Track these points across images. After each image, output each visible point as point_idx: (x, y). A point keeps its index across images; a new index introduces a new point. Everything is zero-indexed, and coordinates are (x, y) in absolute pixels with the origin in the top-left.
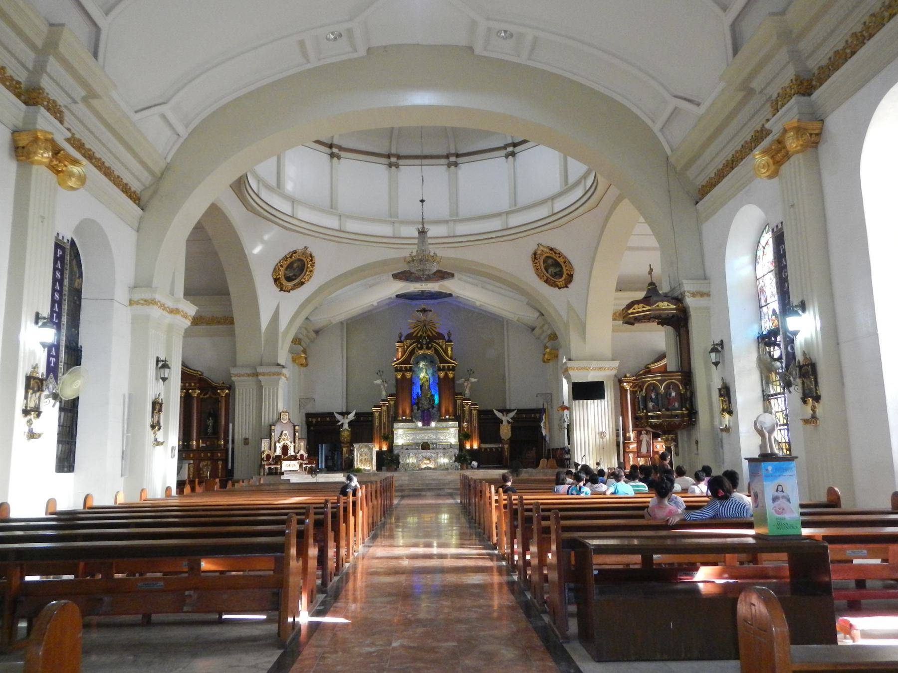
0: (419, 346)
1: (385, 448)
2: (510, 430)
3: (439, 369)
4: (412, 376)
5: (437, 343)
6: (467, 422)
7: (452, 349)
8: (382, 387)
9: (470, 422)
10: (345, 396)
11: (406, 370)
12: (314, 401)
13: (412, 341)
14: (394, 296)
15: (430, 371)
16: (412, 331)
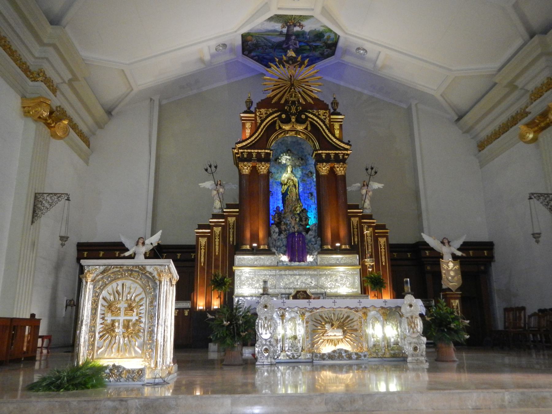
0: (284, 116)
1: (216, 304)
2: (459, 272)
3: (319, 159)
4: (269, 172)
5: (312, 114)
6: (371, 257)
7: (341, 126)
8: (215, 192)
9: (376, 257)
10: (150, 215)
11: (260, 159)
12: (68, 199)
13: (270, 111)
14: (239, 42)
15: (299, 173)
16: (271, 94)
